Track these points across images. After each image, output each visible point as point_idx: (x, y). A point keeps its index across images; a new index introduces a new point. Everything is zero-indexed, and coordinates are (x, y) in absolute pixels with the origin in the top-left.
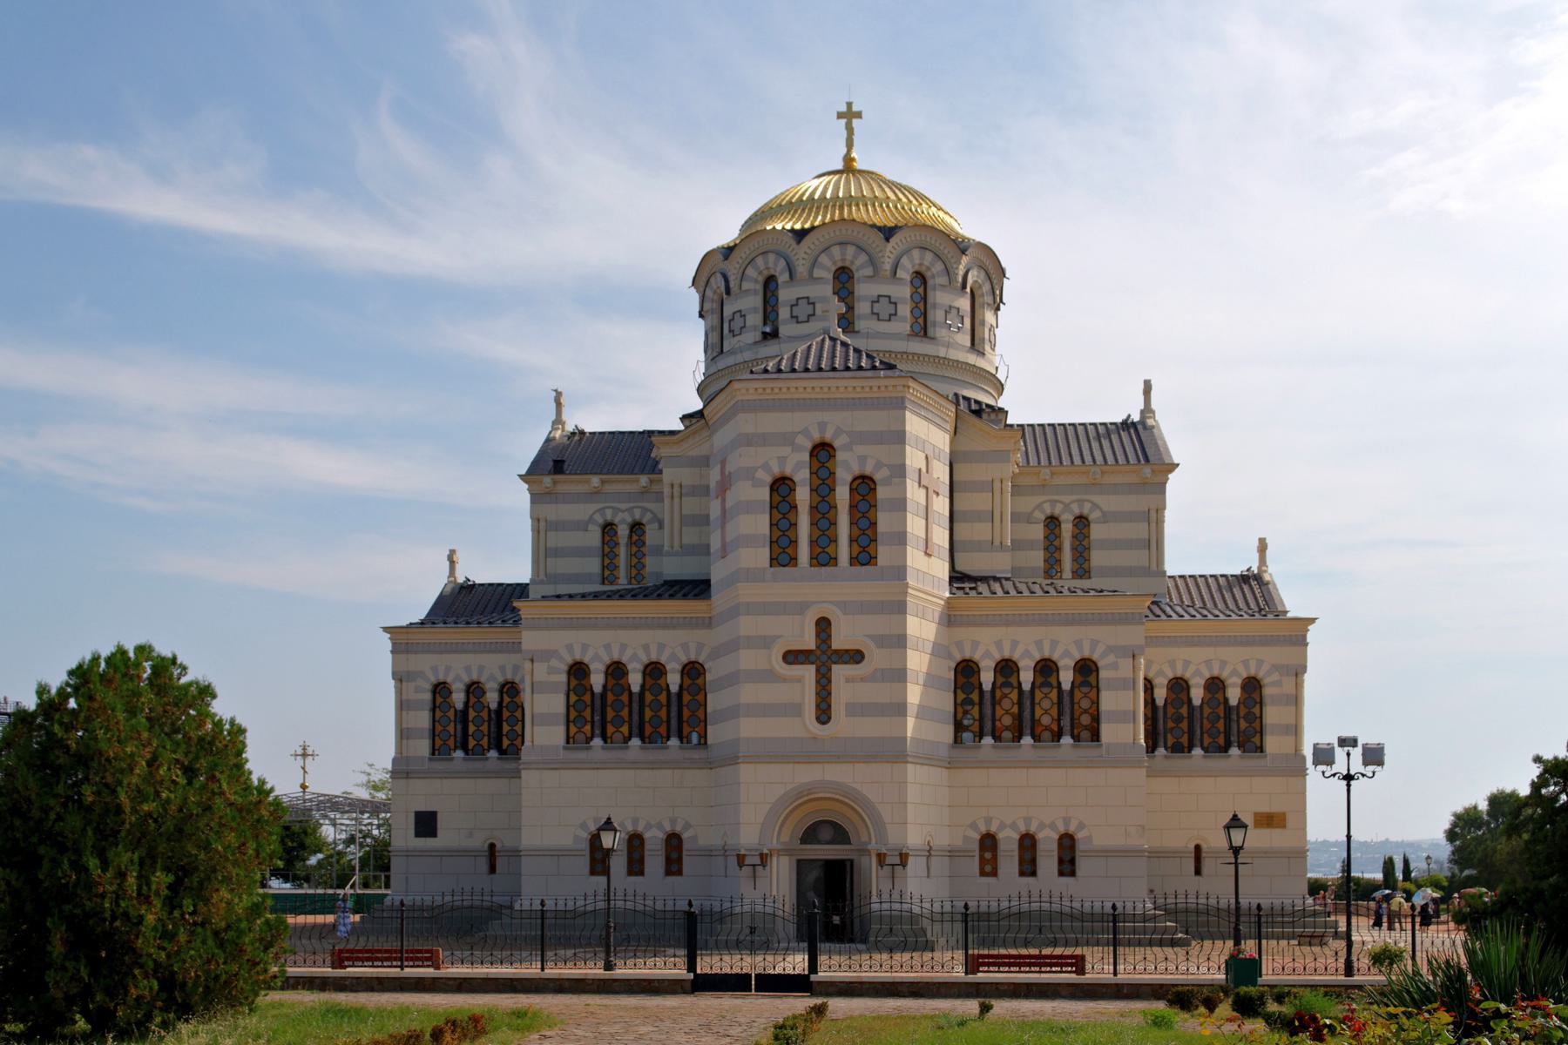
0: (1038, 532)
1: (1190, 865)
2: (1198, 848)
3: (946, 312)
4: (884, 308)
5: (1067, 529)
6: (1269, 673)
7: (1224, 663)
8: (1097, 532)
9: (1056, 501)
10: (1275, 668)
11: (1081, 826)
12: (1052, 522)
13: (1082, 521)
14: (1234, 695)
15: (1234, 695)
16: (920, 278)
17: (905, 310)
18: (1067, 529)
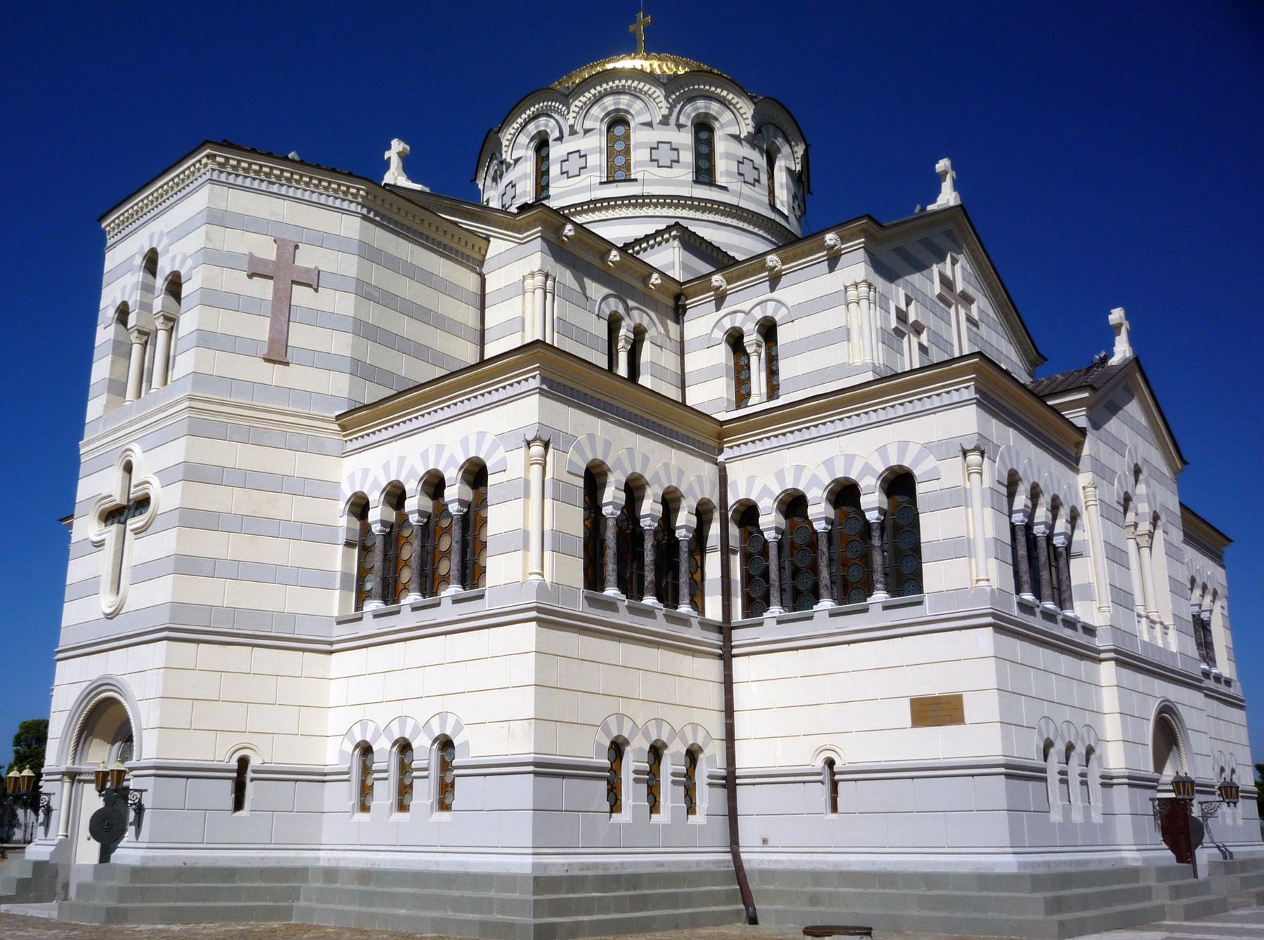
0: (721, 354)
1: (823, 791)
2: (830, 763)
3: (652, 149)
4: (575, 162)
5: (751, 339)
6: (919, 459)
7: (850, 459)
8: (784, 335)
9: (735, 312)
10: (927, 447)
11: (459, 727)
12: (735, 340)
13: (768, 330)
14: (872, 502)
15: (872, 502)
16: (617, 121)
17: (597, 160)
18: (751, 339)
